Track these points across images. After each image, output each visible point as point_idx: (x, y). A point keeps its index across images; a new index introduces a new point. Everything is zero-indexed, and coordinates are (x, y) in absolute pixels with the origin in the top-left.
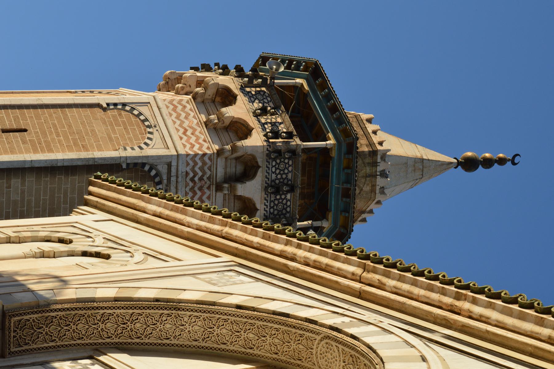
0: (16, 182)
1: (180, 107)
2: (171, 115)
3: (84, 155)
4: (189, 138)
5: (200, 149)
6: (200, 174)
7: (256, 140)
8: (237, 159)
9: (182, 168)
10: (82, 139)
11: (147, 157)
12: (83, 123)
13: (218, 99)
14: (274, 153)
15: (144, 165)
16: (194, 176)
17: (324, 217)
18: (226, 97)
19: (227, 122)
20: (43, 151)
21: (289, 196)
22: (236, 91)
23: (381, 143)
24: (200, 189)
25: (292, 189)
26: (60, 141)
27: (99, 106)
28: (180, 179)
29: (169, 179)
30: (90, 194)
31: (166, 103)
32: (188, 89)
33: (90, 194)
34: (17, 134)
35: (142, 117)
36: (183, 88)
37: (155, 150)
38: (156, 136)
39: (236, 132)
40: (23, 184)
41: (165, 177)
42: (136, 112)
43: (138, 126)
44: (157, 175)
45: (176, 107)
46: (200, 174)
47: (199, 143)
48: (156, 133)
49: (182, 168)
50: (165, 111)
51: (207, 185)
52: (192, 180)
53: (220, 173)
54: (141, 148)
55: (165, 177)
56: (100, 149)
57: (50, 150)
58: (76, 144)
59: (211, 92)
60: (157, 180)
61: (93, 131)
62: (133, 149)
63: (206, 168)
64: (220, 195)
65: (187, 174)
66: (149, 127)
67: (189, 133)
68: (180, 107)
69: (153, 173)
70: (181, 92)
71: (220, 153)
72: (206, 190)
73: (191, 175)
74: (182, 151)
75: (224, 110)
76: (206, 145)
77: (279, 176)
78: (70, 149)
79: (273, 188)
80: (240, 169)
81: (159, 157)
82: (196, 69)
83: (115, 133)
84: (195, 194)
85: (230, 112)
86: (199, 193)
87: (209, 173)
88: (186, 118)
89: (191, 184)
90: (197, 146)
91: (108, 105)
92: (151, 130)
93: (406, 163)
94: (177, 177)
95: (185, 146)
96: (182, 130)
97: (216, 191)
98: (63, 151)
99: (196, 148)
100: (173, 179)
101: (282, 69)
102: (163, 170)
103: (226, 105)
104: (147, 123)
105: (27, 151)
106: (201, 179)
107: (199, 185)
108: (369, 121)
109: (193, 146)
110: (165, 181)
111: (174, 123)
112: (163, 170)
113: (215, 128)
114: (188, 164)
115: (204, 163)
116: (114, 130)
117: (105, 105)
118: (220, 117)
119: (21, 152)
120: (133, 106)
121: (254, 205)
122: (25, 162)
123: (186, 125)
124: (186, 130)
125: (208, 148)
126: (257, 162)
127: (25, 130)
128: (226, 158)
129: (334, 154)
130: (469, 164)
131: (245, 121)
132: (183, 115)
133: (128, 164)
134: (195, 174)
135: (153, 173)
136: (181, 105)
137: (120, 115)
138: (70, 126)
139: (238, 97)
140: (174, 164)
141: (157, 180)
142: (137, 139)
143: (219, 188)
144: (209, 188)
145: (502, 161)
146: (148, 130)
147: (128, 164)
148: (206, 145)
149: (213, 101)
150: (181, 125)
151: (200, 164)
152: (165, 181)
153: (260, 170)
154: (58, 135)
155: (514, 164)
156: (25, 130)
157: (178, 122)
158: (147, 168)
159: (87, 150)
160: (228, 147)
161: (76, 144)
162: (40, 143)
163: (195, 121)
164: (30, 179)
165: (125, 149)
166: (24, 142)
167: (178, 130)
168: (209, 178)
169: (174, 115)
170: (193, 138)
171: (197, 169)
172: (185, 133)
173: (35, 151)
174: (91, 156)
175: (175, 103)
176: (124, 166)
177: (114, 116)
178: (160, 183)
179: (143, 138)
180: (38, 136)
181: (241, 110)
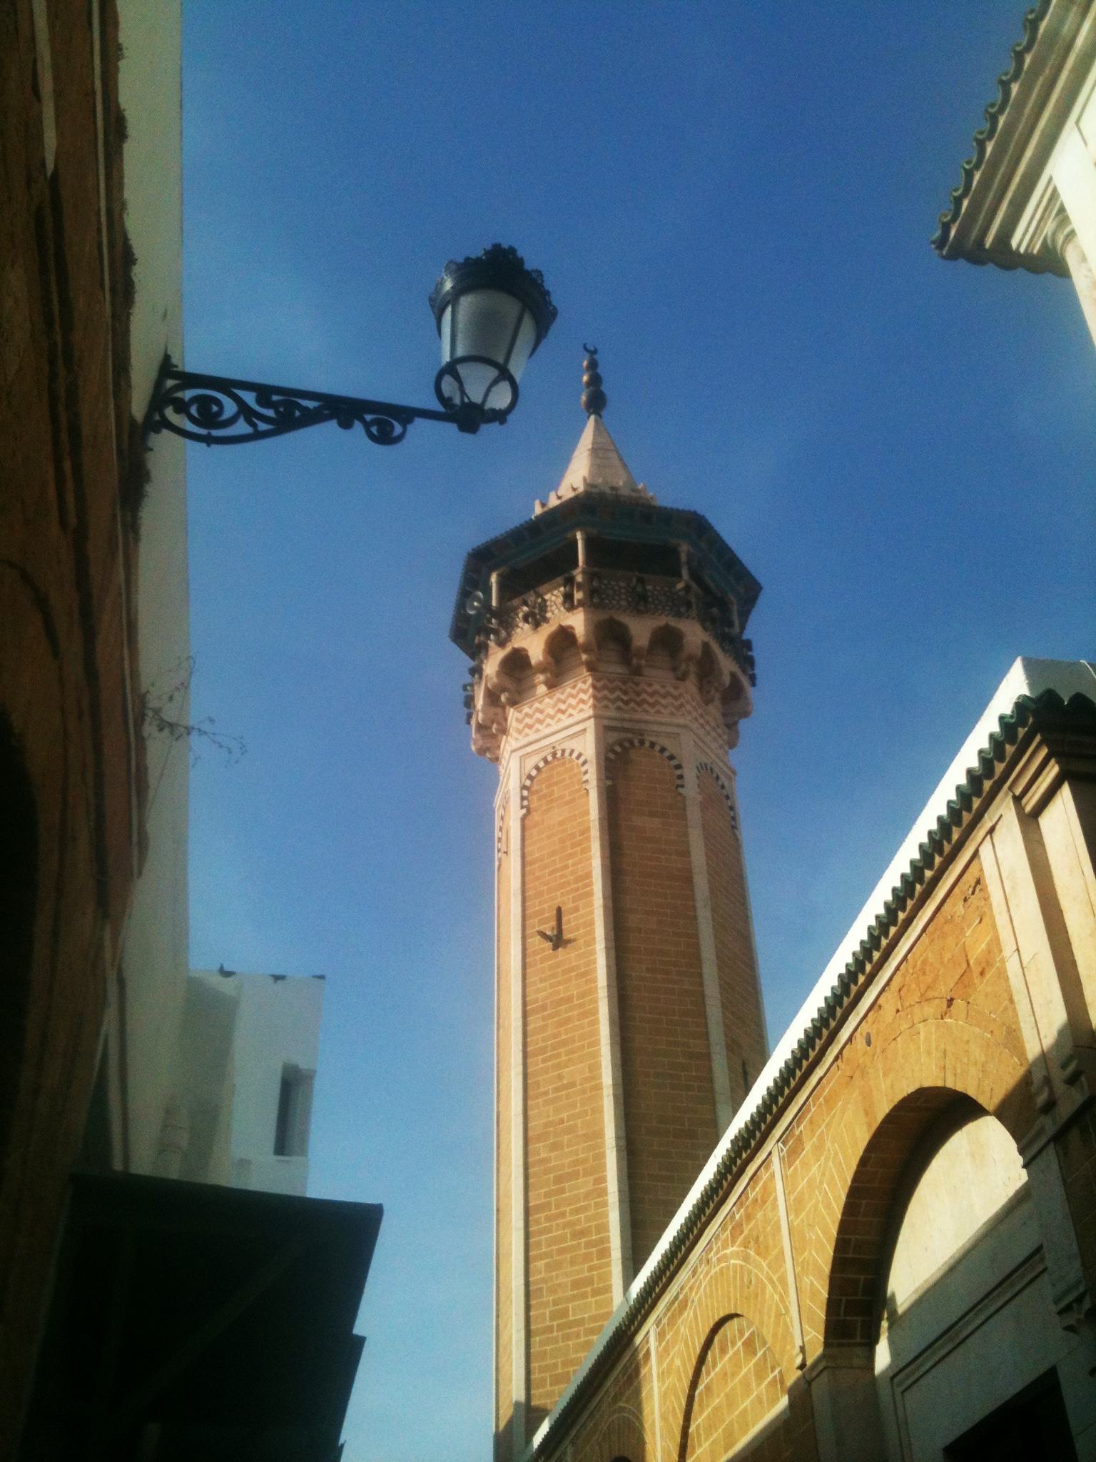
2: (538, 730)
3: (595, 832)
4: (570, 706)
5: (585, 692)
6: (618, 693)
7: (577, 622)
8: (599, 647)
9: (613, 714)
10: (572, 836)
11: (598, 754)
12: (549, 837)
14: (595, 600)
15: (607, 759)
16: (622, 700)
17: (675, 552)
18: (517, 664)
19: (550, 659)
20: (590, 884)
21: (649, 587)
22: (508, 649)
23: (574, 489)
24: (638, 694)
25: (641, 581)
26: (574, 865)
27: (523, 819)
28: (626, 716)
30: (1019, 246)
31: (520, 737)
33: (1019, 246)
34: (564, 920)
35: (541, 764)
36: (499, 724)
37: (587, 746)
38: (568, 746)
41: (623, 735)
42: (534, 773)
43: (553, 768)
44: (621, 745)
48: (563, 746)
49: (613, 714)
50: (533, 737)
52: (626, 703)
53: (619, 669)
54: (585, 762)
55: (623, 735)
56: (587, 813)
57: (588, 875)
58: (580, 843)
59: (508, 683)
60: (627, 745)
61: (560, 824)
62: (586, 772)
63: (610, 686)
64: (646, 671)
65: (619, 708)
66: (554, 755)
67: (563, 707)
68: (527, 721)
69: (618, 749)
71: (592, 668)
72: (640, 688)
73: (620, 704)
74: (591, 712)
75: (533, 662)
76: (580, 685)
78: (588, 849)
79: (641, 604)
81: (598, 740)
82: (469, 716)
84: (644, 701)
86: (644, 696)
87: (618, 683)
88: (541, 712)
89: (632, 705)
90: (582, 696)
91: (522, 807)
93: (599, 466)
94: (623, 720)
95: (581, 710)
96: (560, 716)
97: (641, 675)
98: (590, 858)
99: (584, 697)
100: (626, 725)
101: (480, 594)
102: (613, 736)
104: (550, 758)
105: (591, 904)
106: (625, 693)
107: (633, 696)
108: (543, 505)
109: (582, 701)
110: (629, 735)
111: (549, 725)
112: (613, 736)
117: (524, 811)
118: (542, 669)
119: (592, 913)
120: (524, 777)
122: (605, 906)
123: (552, 712)
125: (584, 682)
127: (559, 910)
128: (598, 660)
129: (594, 531)
130: (597, 403)
132: (538, 715)
133: (607, 778)
134: (619, 699)
135: (618, 749)
137: (537, 792)
138: (554, 853)
139: (516, 646)
140: (606, 722)
141: (627, 745)
142: (572, 768)
143: (637, 671)
144: (637, 684)
145: (593, 365)
146: (559, 755)
147: (607, 778)
148: (580, 685)
150: (552, 717)
151: (606, 692)
152: (629, 735)
153: (616, 617)
154: (567, 867)
155: (595, 352)
156: (559, 910)
157: (549, 721)
158: (612, 756)
159: (588, 829)
160: (584, 657)
161: (580, 843)
162: (578, 889)
163: (547, 700)
165: (587, 781)
166: (576, 909)
167: (560, 720)
168: (624, 683)
169: (538, 726)
170: (573, 701)
171: (613, 696)
172: (563, 712)
173: (590, 894)
174: (597, 823)
177: (539, 799)
178: (631, 742)
179: (571, 761)
180: (568, 893)
181: (533, 643)
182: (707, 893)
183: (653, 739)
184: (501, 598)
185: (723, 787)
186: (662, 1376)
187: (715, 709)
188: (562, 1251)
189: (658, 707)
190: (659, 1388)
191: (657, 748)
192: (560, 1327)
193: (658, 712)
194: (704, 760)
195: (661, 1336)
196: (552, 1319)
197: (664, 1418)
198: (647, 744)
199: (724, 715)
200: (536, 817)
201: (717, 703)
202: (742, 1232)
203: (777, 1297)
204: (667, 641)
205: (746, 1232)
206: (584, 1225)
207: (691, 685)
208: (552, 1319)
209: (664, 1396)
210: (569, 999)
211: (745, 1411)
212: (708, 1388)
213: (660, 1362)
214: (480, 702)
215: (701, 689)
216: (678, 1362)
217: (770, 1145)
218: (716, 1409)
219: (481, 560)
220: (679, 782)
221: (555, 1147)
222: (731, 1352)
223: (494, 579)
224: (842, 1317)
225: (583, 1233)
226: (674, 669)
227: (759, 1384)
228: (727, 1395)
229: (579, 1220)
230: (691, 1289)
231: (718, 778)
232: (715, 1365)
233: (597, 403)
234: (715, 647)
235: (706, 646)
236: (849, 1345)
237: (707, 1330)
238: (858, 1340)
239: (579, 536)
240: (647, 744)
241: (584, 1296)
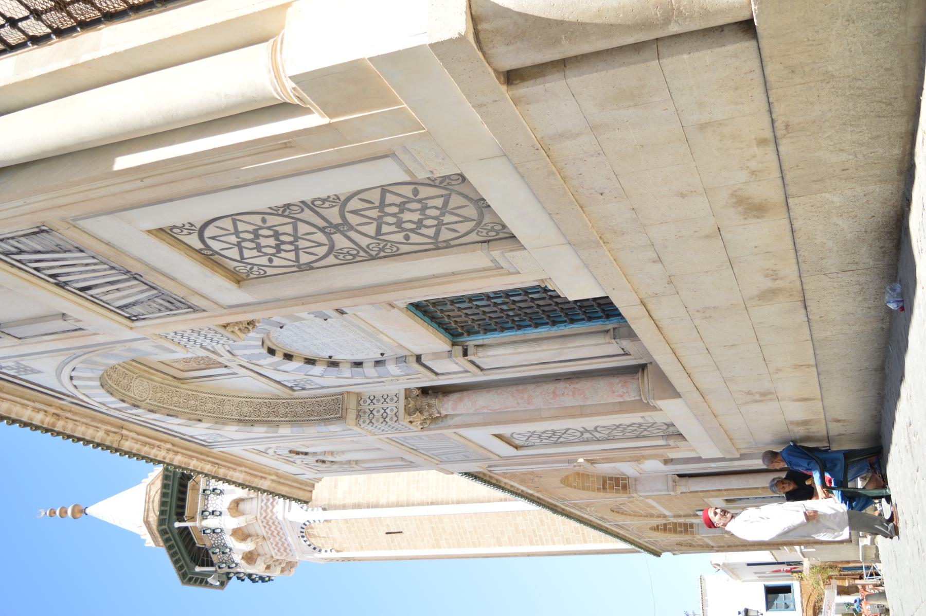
0: (393, 499)
1: (282, 550)
8: (243, 514)
18: (250, 557)
19: (249, 539)
32: (277, 563)
45: (285, 550)
46: (269, 504)
67: (276, 533)
68: (282, 550)
80: (242, 506)
85: (248, 546)
103: (250, 552)
115: (266, 511)
123: (278, 538)
124: (278, 534)
129: (175, 517)
149: (259, 555)
164: (383, 501)
166: (388, 525)
170: (273, 528)
184: (212, 565)
200: (336, 546)
210: (433, 528)
219: (188, 578)
223: (198, 569)
225: (541, 521)
233: (80, 511)
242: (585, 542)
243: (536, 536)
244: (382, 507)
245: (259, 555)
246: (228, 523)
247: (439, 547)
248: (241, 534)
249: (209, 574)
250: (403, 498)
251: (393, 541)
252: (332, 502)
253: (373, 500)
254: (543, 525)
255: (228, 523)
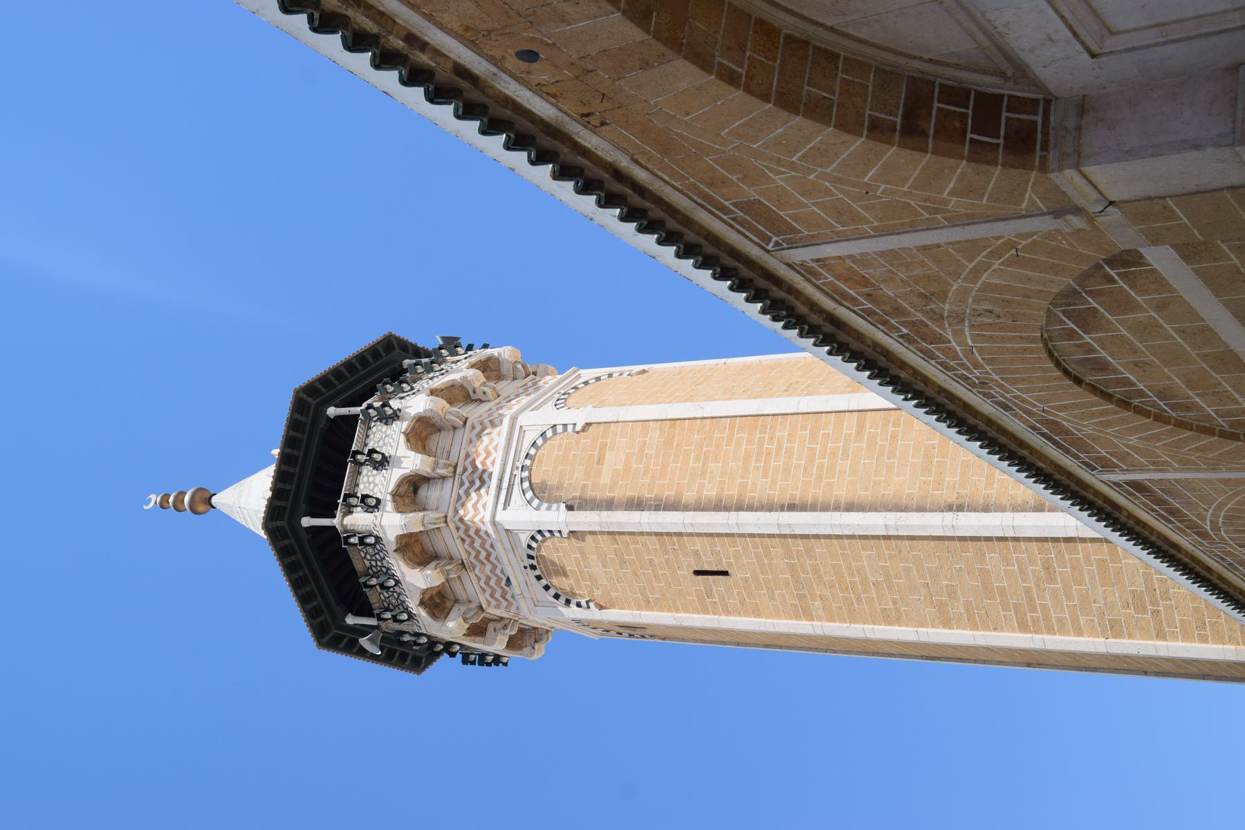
0: (711, 492)
1: (498, 595)
8: (424, 509)
13: (448, 604)
18: (438, 603)
19: (433, 564)
29: (510, 487)
34: (707, 568)
39: (423, 550)
40: (702, 486)
47: (469, 536)
51: (467, 474)
67: (483, 554)
68: (498, 595)
70: (506, 622)
77: (371, 479)
83: (576, 559)
88: (489, 579)
92: (531, 562)
100: (505, 485)
110: (517, 480)
113: (451, 558)
114: (484, 506)
116: (578, 564)
121: (408, 440)
123: (489, 567)
126: (394, 501)
127: (697, 573)
129: (303, 506)
131: (407, 564)
132: (492, 583)
136: (496, 599)
140: (500, 506)
146: (534, 562)
147: (558, 509)
149: (457, 601)
150: (495, 567)
152: (517, 480)
154: (651, 561)
156: (697, 573)
164: (689, 496)
172: (489, 555)
175: (504, 603)
176: (563, 506)
182: (688, 405)
183: (523, 455)
184: (370, 614)
185: (586, 383)
186: (1160, 466)
187: (505, 387)
188: (1069, 597)
189: (491, 448)
190: (1176, 470)
191: (533, 452)
192: (1154, 602)
193: (495, 448)
194: (553, 402)
195: (1107, 465)
196: (1144, 611)
197: (1214, 467)
198: (528, 462)
199: (515, 379)
201: (501, 385)
202: (922, 322)
203: (996, 264)
204: (423, 433)
205: (920, 316)
206: (1039, 567)
207: (474, 413)
208: (1144, 611)
209: (1186, 464)
210: (792, 567)
211: (1181, 332)
212: (1162, 395)
213: (1141, 469)
214: (478, 645)
215: (481, 401)
216: (1133, 440)
217: (774, 264)
218: (1189, 384)
219: (333, 636)
220: (570, 428)
221: (951, 591)
222: (1103, 354)
223: (351, 620)
224: (1001, 141)
225: (1047, 567)
226: (455, 428)
227: (1137, 307)
228: (1167, 363)
229: (1034, 572)
230: (1029, 413)
231: (576, 388)
232: (1128, 382)
233: (204, 500)
234: (440, 381)
235: (433, 392)
236: (1046, 133)
237: (1077, 389)
238: (1039, 118)
239: (306, 522)
240: (528, 462)
241: (1119, 572)
242: (1161, 635)
243: (1033, 610)
244: (686, 508)
245: (457, 601)
246: (391, 523)
247: (810, 617)
248: (417, 549)
249: (363, 631)
250: (732, 492)
251: (709, 594)
252: (589, 494)
253: (669, 494)
254: (1052, 580)
255: (391, 523)
